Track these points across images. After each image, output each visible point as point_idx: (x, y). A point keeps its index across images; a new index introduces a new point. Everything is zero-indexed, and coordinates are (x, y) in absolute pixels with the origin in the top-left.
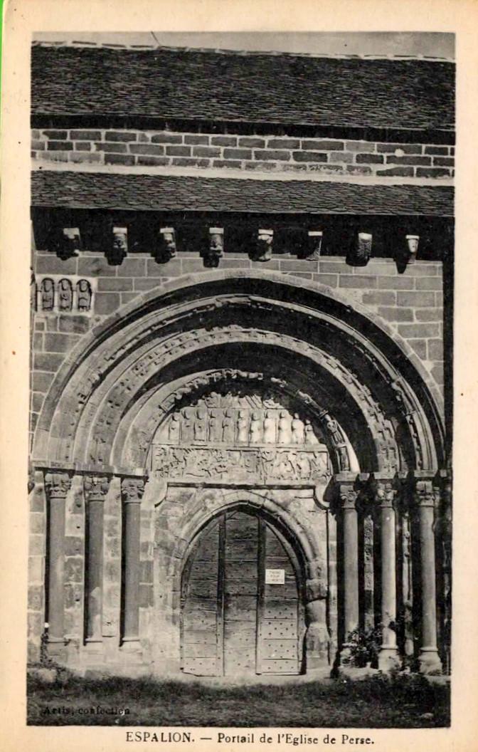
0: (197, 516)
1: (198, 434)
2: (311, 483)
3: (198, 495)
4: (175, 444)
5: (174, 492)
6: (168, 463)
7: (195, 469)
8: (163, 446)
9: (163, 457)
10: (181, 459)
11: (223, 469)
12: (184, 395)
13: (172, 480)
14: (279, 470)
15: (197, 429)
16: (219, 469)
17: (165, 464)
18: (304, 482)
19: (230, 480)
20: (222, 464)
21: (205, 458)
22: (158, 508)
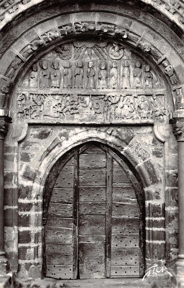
0: (54, 151)
1: (53, 82)
2: (151, 121)
3: (56, 133)
4: (33, 90)
5: (35, 132)
6: (28, 107)
7: (52, 112)
8: (24, 93)
9: (24, 101)
10: (39, 103)
11: (75, 111)
12: (39, 46)
13: (32, 121)
14: (125, 112)
15: (52, 77)
16: (72, 111)
17: (25, 107)
18: (144, 121)
19: (81, 121)
20: (74, 106)
21: (59, 102)
22: (21, 145)
